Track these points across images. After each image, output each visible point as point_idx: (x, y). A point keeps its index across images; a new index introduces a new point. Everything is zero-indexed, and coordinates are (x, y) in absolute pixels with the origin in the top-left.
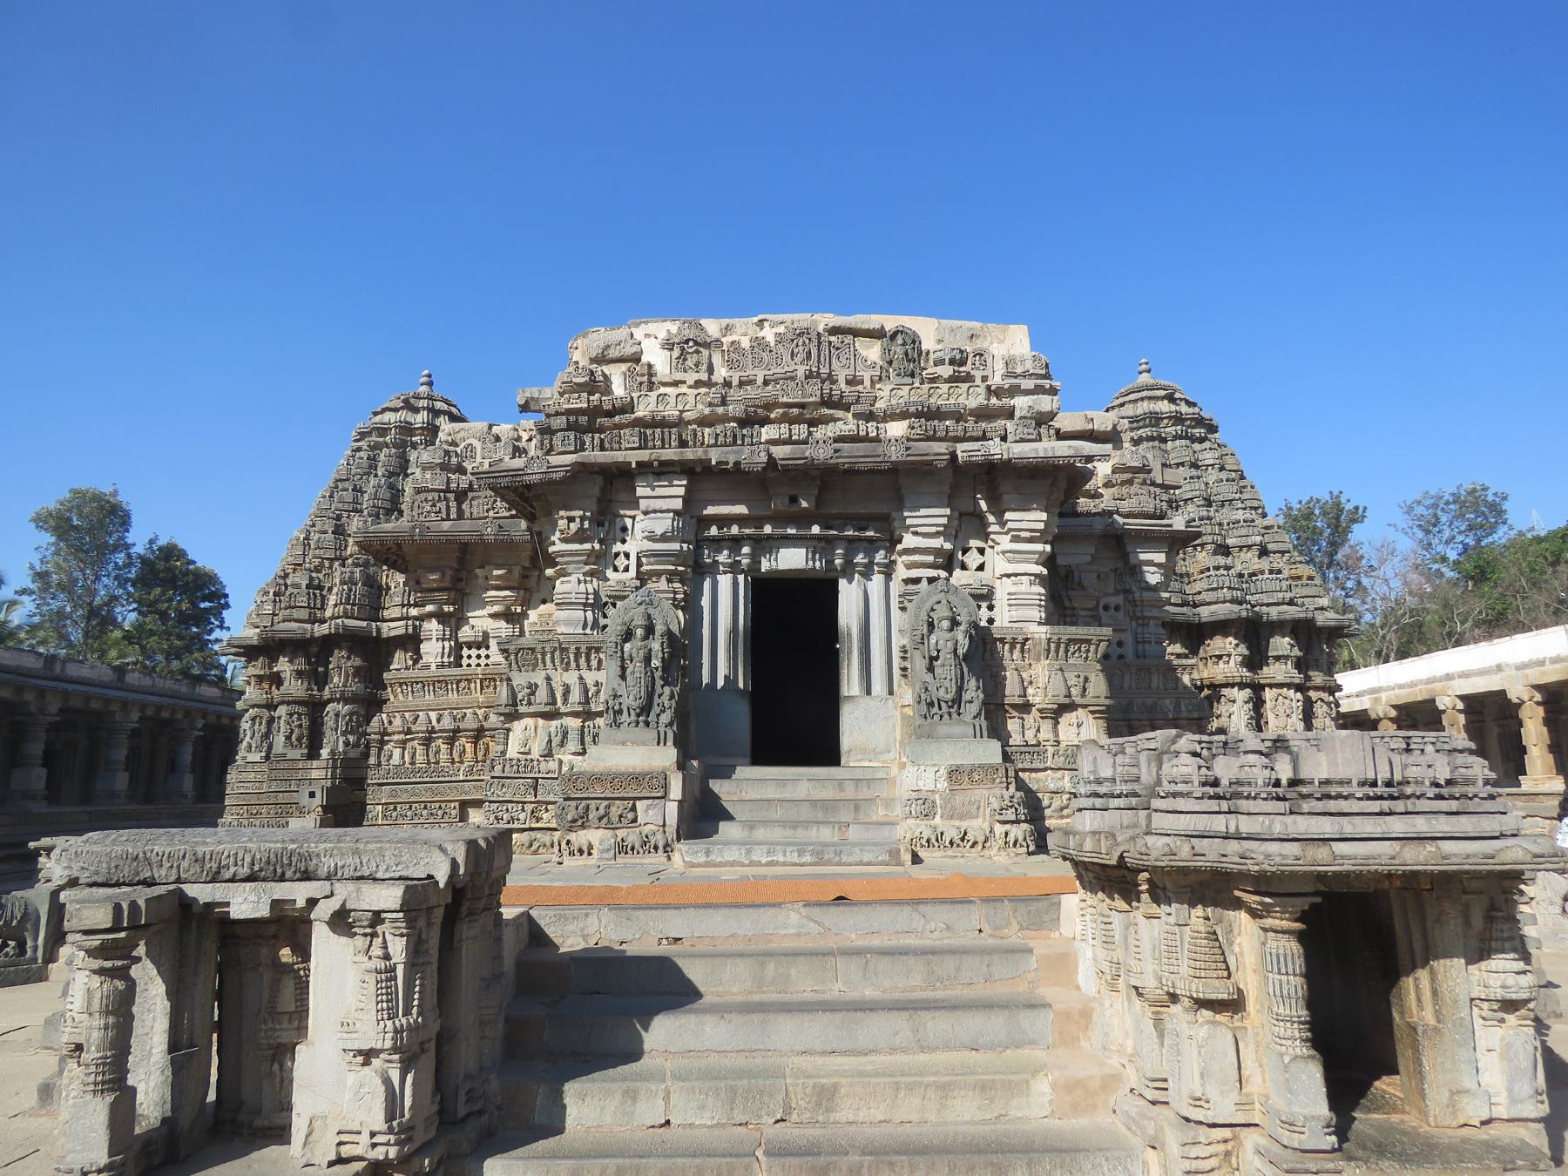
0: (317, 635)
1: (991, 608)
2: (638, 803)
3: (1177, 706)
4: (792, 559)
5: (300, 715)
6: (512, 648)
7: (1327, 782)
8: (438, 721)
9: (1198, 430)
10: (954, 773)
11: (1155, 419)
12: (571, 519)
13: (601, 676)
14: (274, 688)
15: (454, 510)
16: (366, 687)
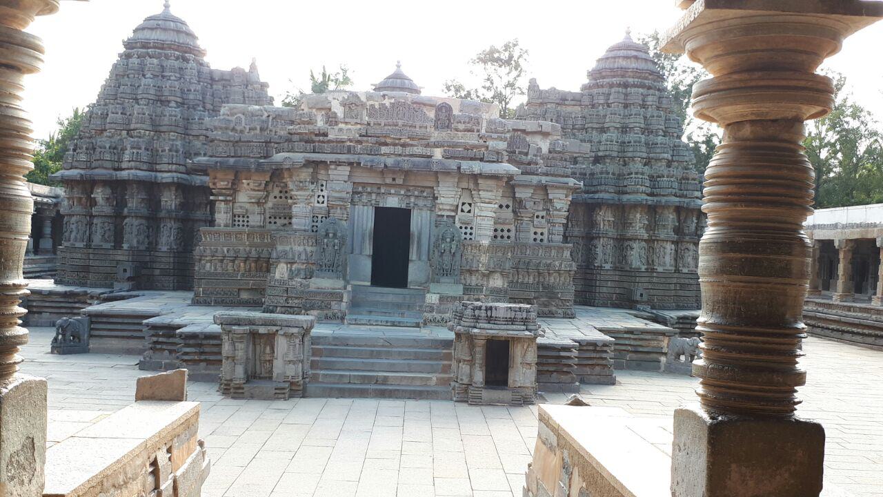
0: (119, 179)
1: (471, 228)
2: (333, 303)
3: (561, 265)
4: (392, 202)
5: (109, 223)
6: (278, 236)
7: (496, 317)
8: (228, 252)
9: (646, 81)
10: (441, 299)
11: (624, 72)
12: (301, 182)
13: (314, 249)
14: (88, 205)
15: (233, 151)
16: (148, 210)
